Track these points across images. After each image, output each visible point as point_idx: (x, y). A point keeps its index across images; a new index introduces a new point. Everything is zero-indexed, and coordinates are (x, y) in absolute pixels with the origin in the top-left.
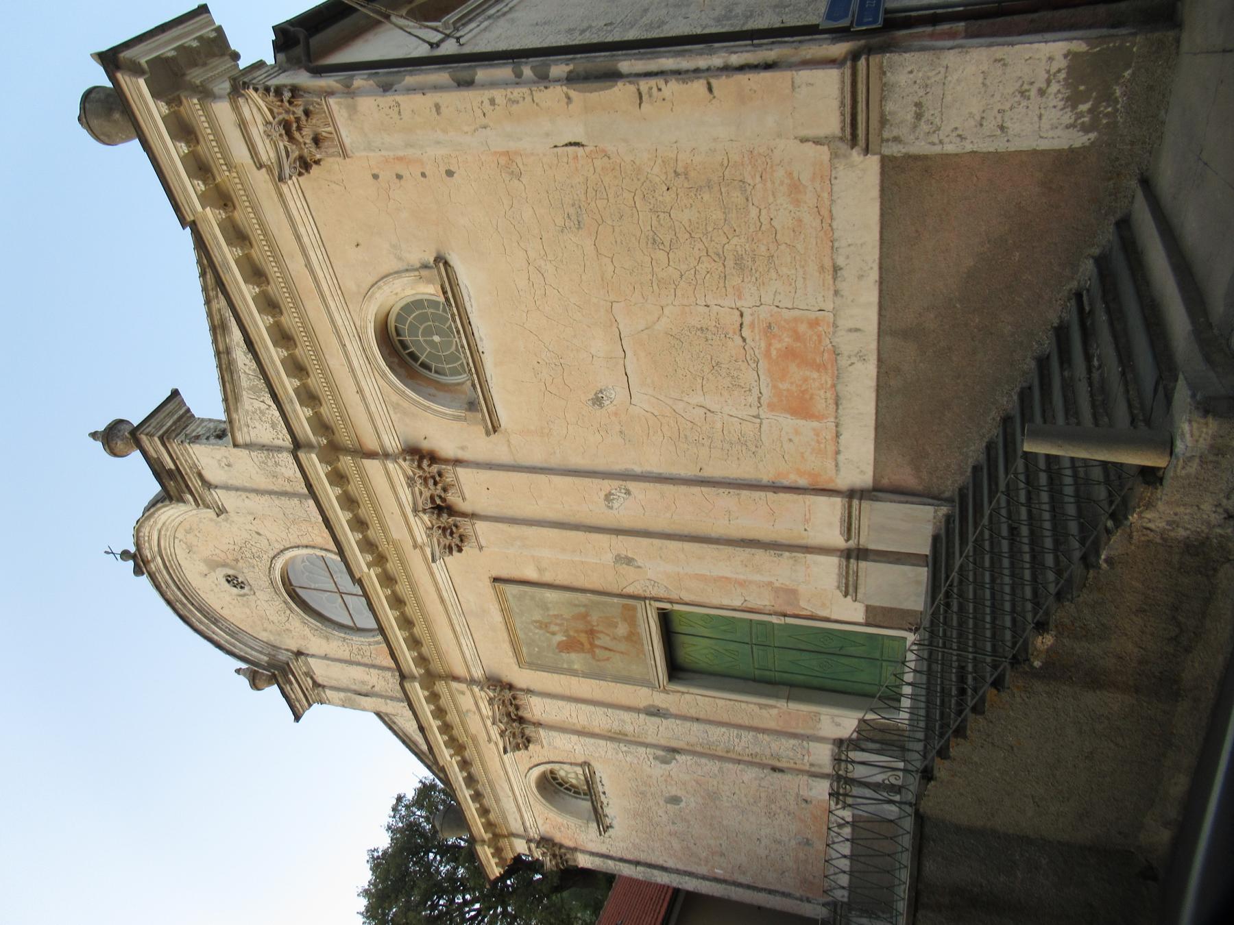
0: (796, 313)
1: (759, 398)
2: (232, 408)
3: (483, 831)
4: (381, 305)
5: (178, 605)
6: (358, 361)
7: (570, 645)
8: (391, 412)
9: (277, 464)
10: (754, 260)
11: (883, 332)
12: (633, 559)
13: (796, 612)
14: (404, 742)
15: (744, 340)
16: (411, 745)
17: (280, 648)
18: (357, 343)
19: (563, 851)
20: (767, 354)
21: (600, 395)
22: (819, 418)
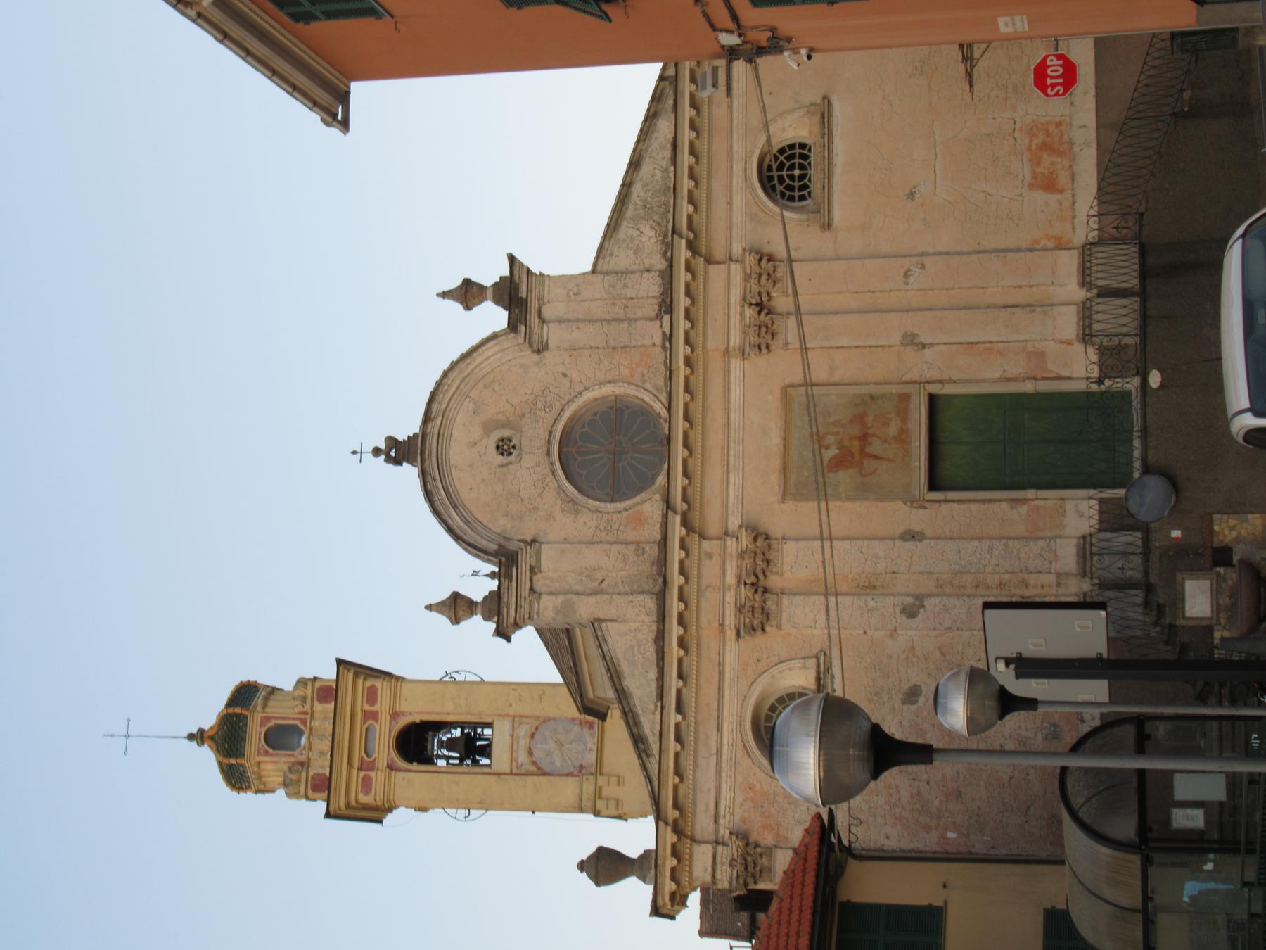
0: (1047, 119)
1: (1023, 181)
2: (608, 237)
3: (670, 802)
4: (762, 149)
5: (429, 479)
6: (738, 180)
7: (839, 463)
8: (747, 223)
9: (625, 285)
10: (1024, 87)
11: (1099, 127)
12: (917, 335)
13: (1045, 375)
14: (608, 670)
15: (1015, 139)
16: (614, 676)
17: (513, 540)
18: (742, 166)
19: (758, 850)
20: (1029, 148)
21: (914, 190)
22: (1061, 192)
